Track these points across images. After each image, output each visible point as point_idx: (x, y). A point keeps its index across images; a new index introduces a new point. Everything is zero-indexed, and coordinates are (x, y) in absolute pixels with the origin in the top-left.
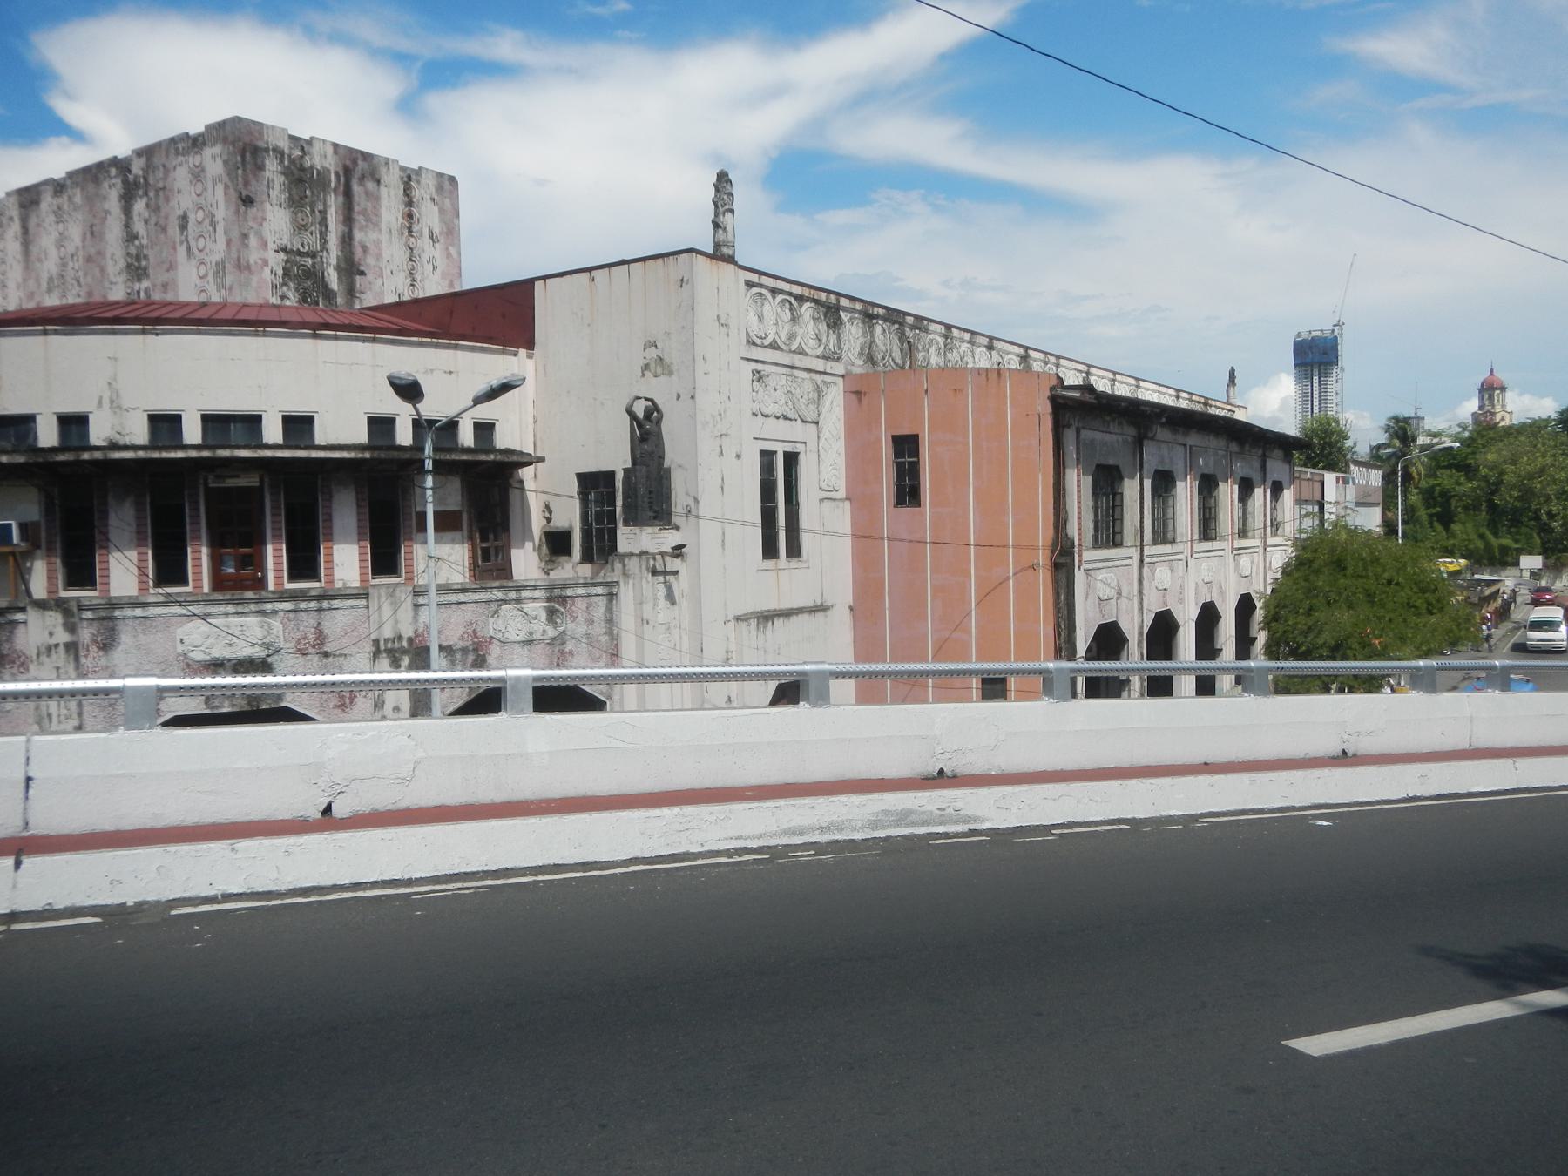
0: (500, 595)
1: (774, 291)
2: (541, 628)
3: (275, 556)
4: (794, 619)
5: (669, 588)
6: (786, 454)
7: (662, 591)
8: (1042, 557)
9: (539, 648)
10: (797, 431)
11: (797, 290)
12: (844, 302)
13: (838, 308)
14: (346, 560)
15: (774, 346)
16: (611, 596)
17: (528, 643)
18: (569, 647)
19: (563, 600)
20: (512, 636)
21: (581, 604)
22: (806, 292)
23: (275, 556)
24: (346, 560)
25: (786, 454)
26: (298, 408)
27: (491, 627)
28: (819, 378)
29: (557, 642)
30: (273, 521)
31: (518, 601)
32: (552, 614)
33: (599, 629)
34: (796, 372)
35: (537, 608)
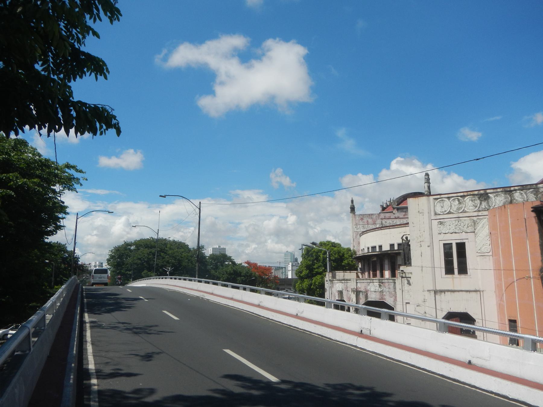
0: (369, 281)
2: (377, 288)
3: (378, 273)
4: (455, 293)
6: (457, 244)
7: (406, 282)
9: (378, 293)
11: (462, 194)
12: (488, 191)
13: (487, 194)
14: (387, 274)
15: (450, 213)
16: (395, 283)
17: (375, 292)
18: (384, 293)
19: (382, 283)
20: (372, 290)
21: (387, 284)
22: (465, 194)
23: (378, 273)
24: (387, 274)
25: (457, 244)
26: (380, 244)
27: (368, 288)
28: (475, 218)
29: (382, 292)
30: (378, 267)
31: (373, 282)
32: (380, 286)
33: (392, 290)
34: (461, 219)
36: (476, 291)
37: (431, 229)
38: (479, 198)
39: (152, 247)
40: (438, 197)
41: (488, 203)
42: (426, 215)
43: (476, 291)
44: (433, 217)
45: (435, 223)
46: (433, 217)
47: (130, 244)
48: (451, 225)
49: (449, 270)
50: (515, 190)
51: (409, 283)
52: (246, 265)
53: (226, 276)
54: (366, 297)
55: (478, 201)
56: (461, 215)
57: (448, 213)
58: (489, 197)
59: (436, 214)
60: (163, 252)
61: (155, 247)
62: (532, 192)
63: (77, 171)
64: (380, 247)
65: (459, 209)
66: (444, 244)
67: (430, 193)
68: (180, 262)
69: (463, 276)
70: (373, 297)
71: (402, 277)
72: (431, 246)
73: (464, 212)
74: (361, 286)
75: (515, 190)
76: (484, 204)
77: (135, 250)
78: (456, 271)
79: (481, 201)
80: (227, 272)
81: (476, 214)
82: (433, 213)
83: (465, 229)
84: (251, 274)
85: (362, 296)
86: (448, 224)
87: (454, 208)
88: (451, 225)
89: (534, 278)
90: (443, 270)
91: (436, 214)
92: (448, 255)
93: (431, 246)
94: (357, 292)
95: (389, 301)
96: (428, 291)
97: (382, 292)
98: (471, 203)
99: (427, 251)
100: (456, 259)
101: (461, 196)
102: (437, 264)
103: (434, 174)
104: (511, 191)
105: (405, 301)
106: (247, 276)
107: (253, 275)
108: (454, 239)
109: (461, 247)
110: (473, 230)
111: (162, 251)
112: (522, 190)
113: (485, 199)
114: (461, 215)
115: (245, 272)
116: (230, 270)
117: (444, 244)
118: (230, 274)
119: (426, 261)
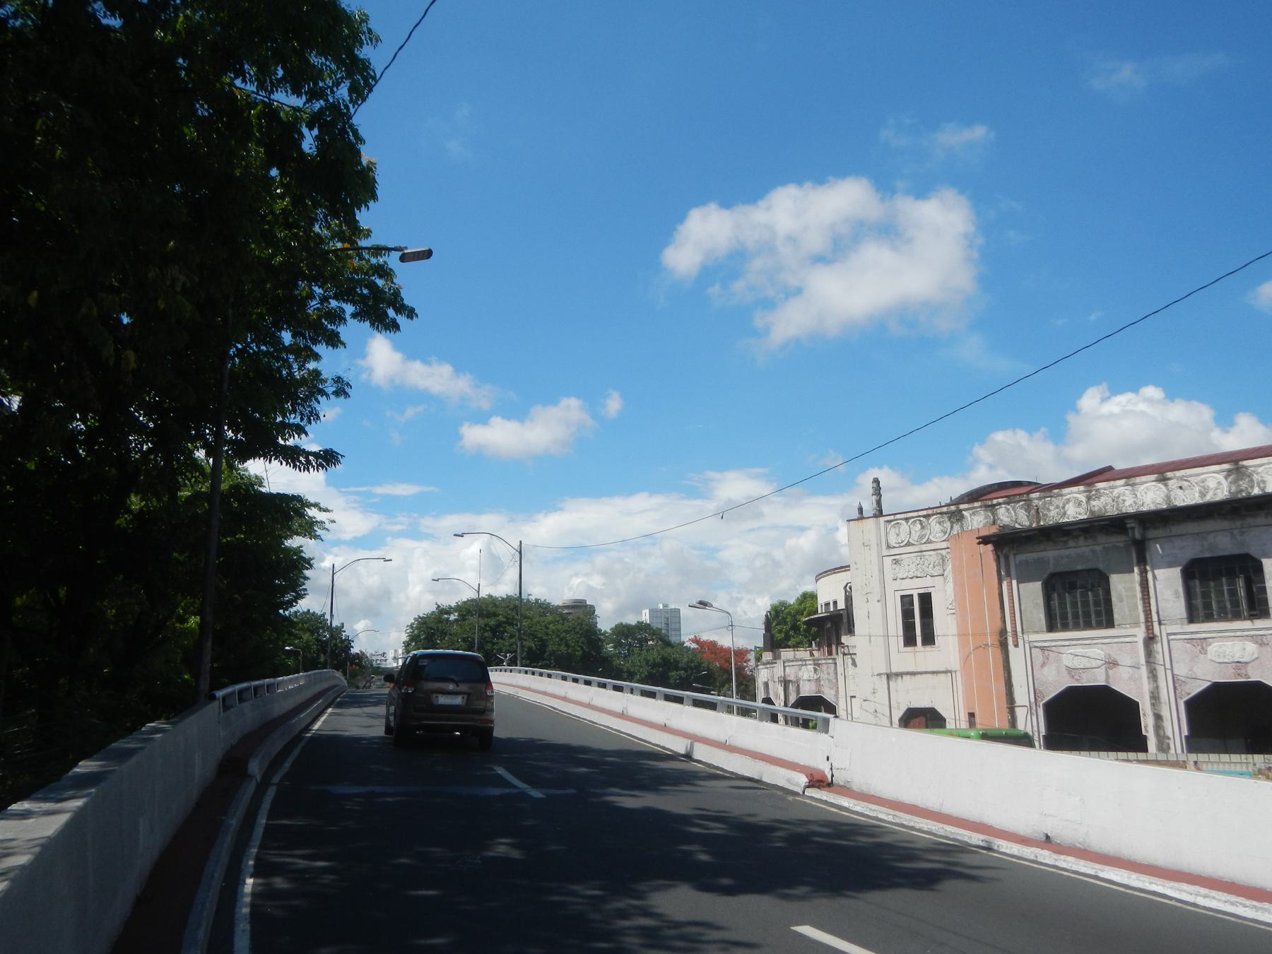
1: (907, 519)
2: (812, 674)
5: (854, 661)
6: (920, 595)
8: (991, 639)
10: (928, 581)
11: (925, 513)
13: (961, 511)
15: (909, 544)
20: (805, 677)
21: (825, 667)
22: (930, 512)
25: (920, 595)
28: (944, 552)
29: (818, 680)
32: (815, 670)
33: (832, 676)
35: (811, 668)
36: (945, 672)
37: (882, 572)
38: (950, 519)
39: (490, 615)
40: (892, 518)
41: (962, 526)
42: (874, 548)
43: (945, 672)
44: (885, 552)
45: (888, 561)
46: (885, 552)
47: (448, 611)
48: (910, 564)
49: (909, 640)
50: (999, 504)
51: (854, 664)
52: (694, 646)
53: (645, 671)
54: (798, 691)
55: (948, 525)
56: (924, 547)
57: (907, 545)
58: (963, 517)
59: (889, 547)
60: (512, 624)
61: (495, 615)
62: (1022, 507)
63: (320, 509)
64: (835, 603)
65: (921, 537)
66: (902, 597)
67: (881, 511)
68: (543, 645)
69: (928, 648)
70: (807, 690)
71: (844, 654)
72: (883, 600)
73: (929, 542)
74: (791, 673)
75: (999, 504)
76: (957, 528)
77: (456, 620)
78: (919, 639)
79: (952, 523)
80: (647, 661)
81: (944, 545)
82: (884, 546)
83: (930, 571)
84: (700, 665)
85: (792, 688)
86: (905, 562)
87: (915, 536)
88: (910, 564)
89: (992, 645)
90: (901, 640)
91: (889, 547)
92: (907, 614)
93: (883, 600)
94: (786, 683)
95: (829, 695)
96: (879, 675)
97: (818, 680)
98: (938, 528)
99: (876, 608)
100: (918, 620)
101: (924, 516)
102: (892, 631)
103: (887, 478)
104: (994, 506)
105: (849, 694)
106: (691, 668)
107: (705, 665)
108: (914, 588)
109: (926, 599)
110: (940, 572)
111: (510, 622)
112: (1008, 504)
113: (958, 520)
114: (924, 547)
115: (686, 660)
116: (654, 656)
117: (902, 597)
118: (654, 665)
119: (875, 626)
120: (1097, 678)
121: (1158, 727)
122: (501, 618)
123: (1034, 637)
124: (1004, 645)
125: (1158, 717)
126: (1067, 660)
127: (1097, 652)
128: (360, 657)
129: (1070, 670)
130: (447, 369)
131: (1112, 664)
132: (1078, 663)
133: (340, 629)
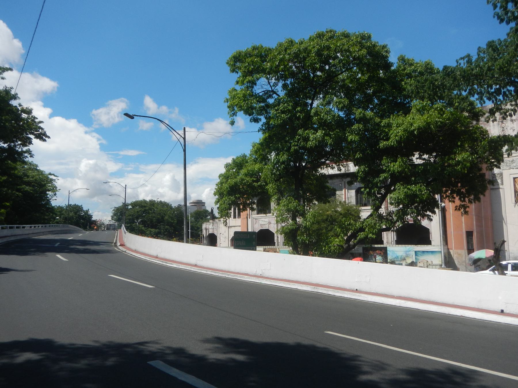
61: (145, 207)
68: (163, 217)
120: (264, 228)
121: (277, 240)
122: (147, 208)
123: (254, 216)
124: (247, 218)
125: (278, 237)
126: (261, 222)
127: (267, 220)
128: (95, 222)
129: (261, 225)
130: (41, 154)
131: (270, 223)
132: (263, 223)
133: (87, 211)
